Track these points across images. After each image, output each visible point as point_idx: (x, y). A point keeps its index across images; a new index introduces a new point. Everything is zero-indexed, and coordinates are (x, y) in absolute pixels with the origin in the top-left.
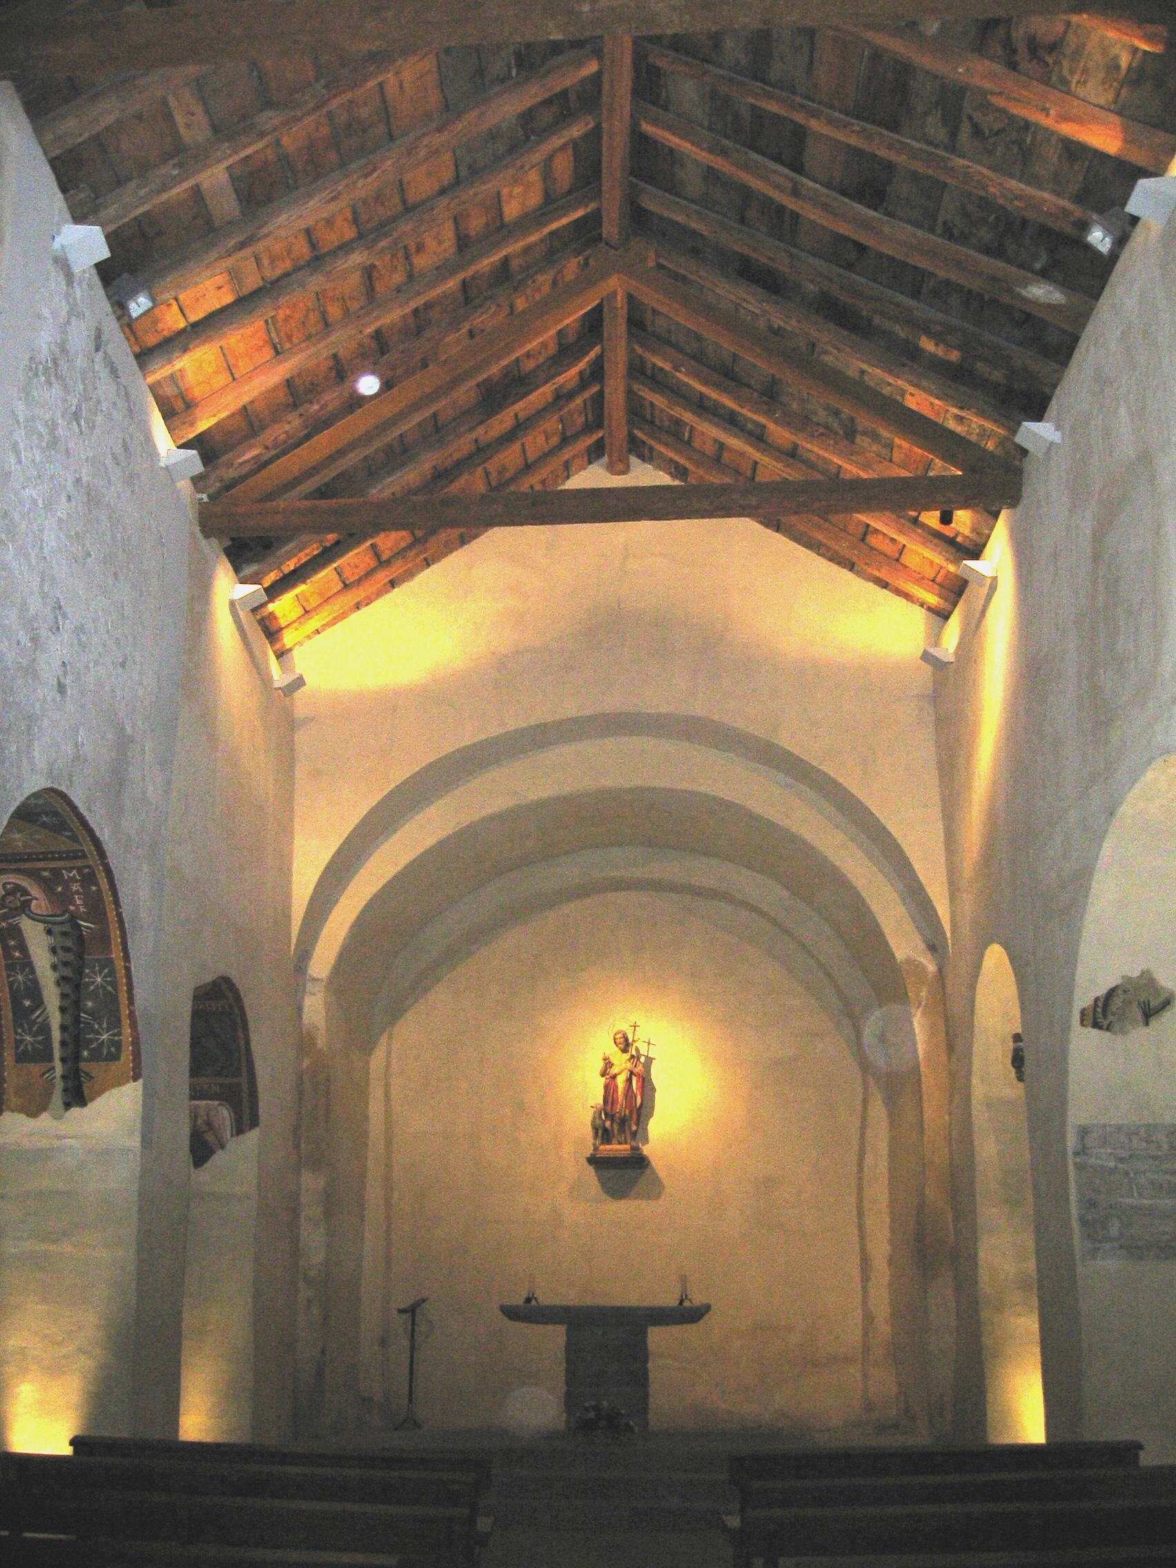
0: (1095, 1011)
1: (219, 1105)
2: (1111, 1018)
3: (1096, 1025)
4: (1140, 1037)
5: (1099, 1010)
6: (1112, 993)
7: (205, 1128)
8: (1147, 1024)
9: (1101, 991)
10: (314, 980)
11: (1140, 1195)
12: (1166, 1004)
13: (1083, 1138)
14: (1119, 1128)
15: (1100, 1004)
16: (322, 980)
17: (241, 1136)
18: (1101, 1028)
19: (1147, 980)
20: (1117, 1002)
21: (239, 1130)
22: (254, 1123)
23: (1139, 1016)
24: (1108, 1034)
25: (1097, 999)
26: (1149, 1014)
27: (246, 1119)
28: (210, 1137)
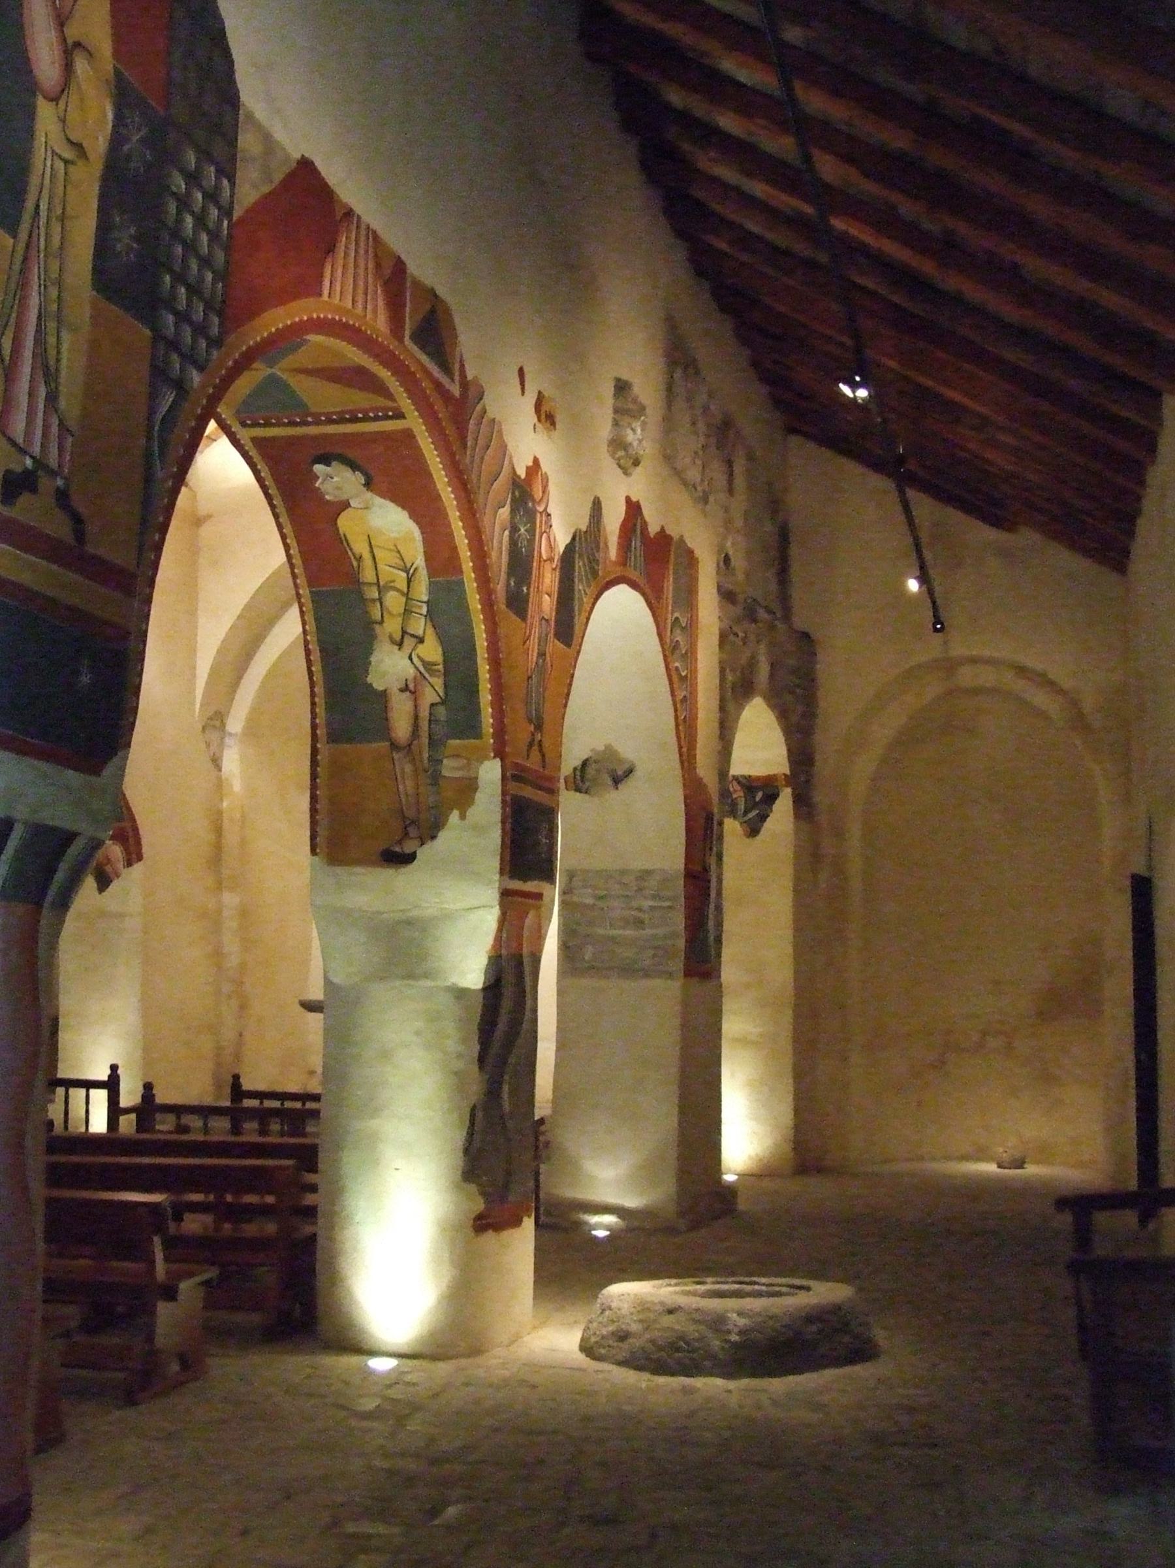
0: (575, 778)
1: (113, 843)
2: (587, 784)
3: (578, 790)
4: (614, 797)
5: (578, 777)
6: (585, 764)
7: (105, 861)
8: (617, 788)
9: (578, 763)
10: (230, 734)
11: (611, 925)
12: (630, 772)
13: (571, 880)
14: (599, 873)
15: (578, 773)
16: (236, 735)
17: (130, 868)
18: (581, 792)
19: (610, 753)
20: (591, 771)
21: (129, 864)
22: (140, 858)
23: (609, 782)
24: (587, 797)
25: (575, 769)
26: (617, 781)
27: (134, 854)
28: (108, 869)
